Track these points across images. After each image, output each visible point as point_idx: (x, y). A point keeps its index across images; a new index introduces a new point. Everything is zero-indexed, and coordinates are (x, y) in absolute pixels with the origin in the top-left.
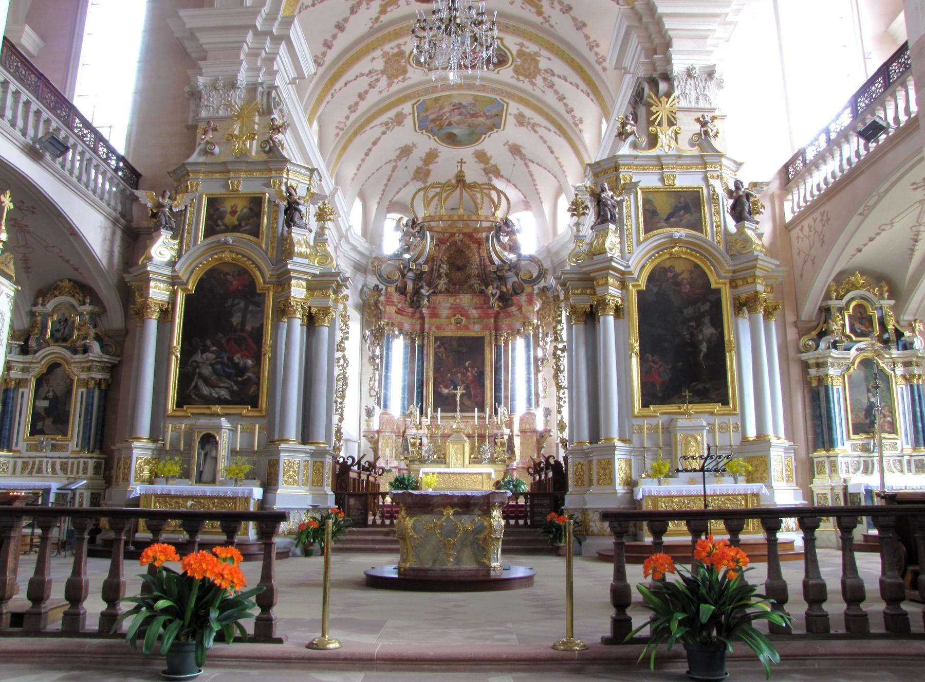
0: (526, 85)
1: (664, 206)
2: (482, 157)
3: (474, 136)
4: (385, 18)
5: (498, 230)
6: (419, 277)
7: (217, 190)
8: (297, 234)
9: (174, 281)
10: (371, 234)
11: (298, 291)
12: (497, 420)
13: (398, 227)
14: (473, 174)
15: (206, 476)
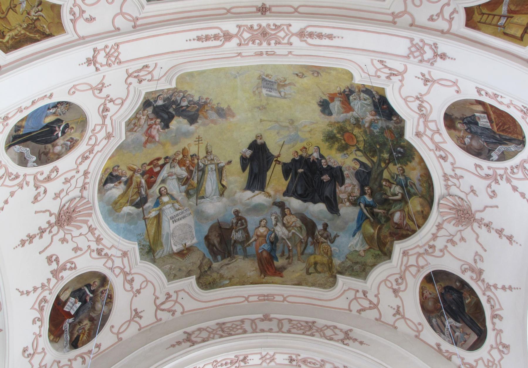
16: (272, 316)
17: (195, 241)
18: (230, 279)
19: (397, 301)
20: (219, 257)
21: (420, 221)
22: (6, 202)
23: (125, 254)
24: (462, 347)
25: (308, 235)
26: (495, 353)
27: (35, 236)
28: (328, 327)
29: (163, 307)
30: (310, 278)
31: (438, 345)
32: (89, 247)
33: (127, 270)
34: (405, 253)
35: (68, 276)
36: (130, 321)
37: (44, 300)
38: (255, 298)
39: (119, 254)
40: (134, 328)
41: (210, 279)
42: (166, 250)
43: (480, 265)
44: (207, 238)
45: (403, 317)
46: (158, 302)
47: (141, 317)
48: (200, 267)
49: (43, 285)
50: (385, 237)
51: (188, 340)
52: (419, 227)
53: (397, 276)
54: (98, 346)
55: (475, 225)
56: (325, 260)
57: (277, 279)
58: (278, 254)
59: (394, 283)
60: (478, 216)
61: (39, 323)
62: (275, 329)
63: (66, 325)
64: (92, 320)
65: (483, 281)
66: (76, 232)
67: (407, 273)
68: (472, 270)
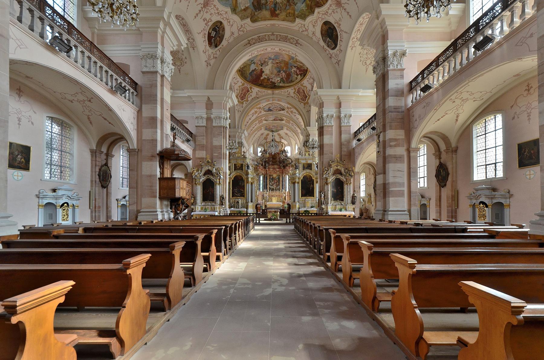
0: (288, 124)
1: (306, 166)
2: (279, 135)
3: (277, 131)
4: (258, 115)
5: (283, 152)
6: (265, 162)
7: (236, 163)
8: (249, 171)
9: (230, 178)
10: (255, 153)
11: (250, 180)
12: (282, 192)
13: (260, 152)
14: (277, 139)
15: (238, 207)
16: (275, 33)
17: (249, 4)
18: (261, 18)
19: (314, 30)
20: (257, 10)
21: (325, 2)
22: (188, 6)
23: (226, 12)
24: (330, 48)
25: (287, 2)
26: (338, 52)
27: (198, 13)
28: (292, 38)
29: (240, 30)
30: (287, 18)
31: (323, 46)
32: (215, 12)
33: (228, 18)
34: (319, 13)
35: (210, 24)
36: (231, 36)
37: (205, 34)
38: (269, 25)
39: (224, 13)
40: (232, 39)
41: (255, 19)
42: (240, 9)
43: (340, 22)
44: (253, 3)
45: (315, 35)
46: (239, 28)
47: (234, 34)
48: (251, 14)
49: (204, 29)
50: (313, 6)
51: (249, 43)
52: (324, 4)
53: (315, 21)
54: (223, 46)
55: (341, 8)
56: (293, 12)
57: (276, 18)
58: (277, 9)
59: (314, 23)
60: (343, 5)
61: (205, 42)
62: (275, 39)
63: (213, 41)
64: (219, 37)
65: (340, 28)
66: (210, 8)
67: (318, 20)
68: (338, 23)
